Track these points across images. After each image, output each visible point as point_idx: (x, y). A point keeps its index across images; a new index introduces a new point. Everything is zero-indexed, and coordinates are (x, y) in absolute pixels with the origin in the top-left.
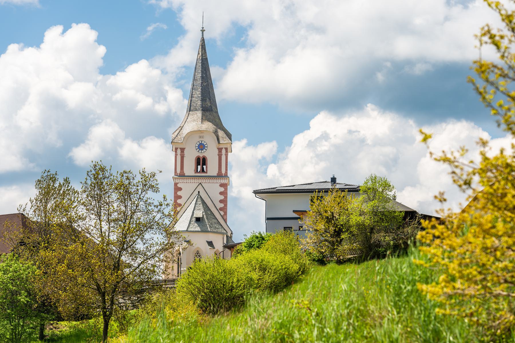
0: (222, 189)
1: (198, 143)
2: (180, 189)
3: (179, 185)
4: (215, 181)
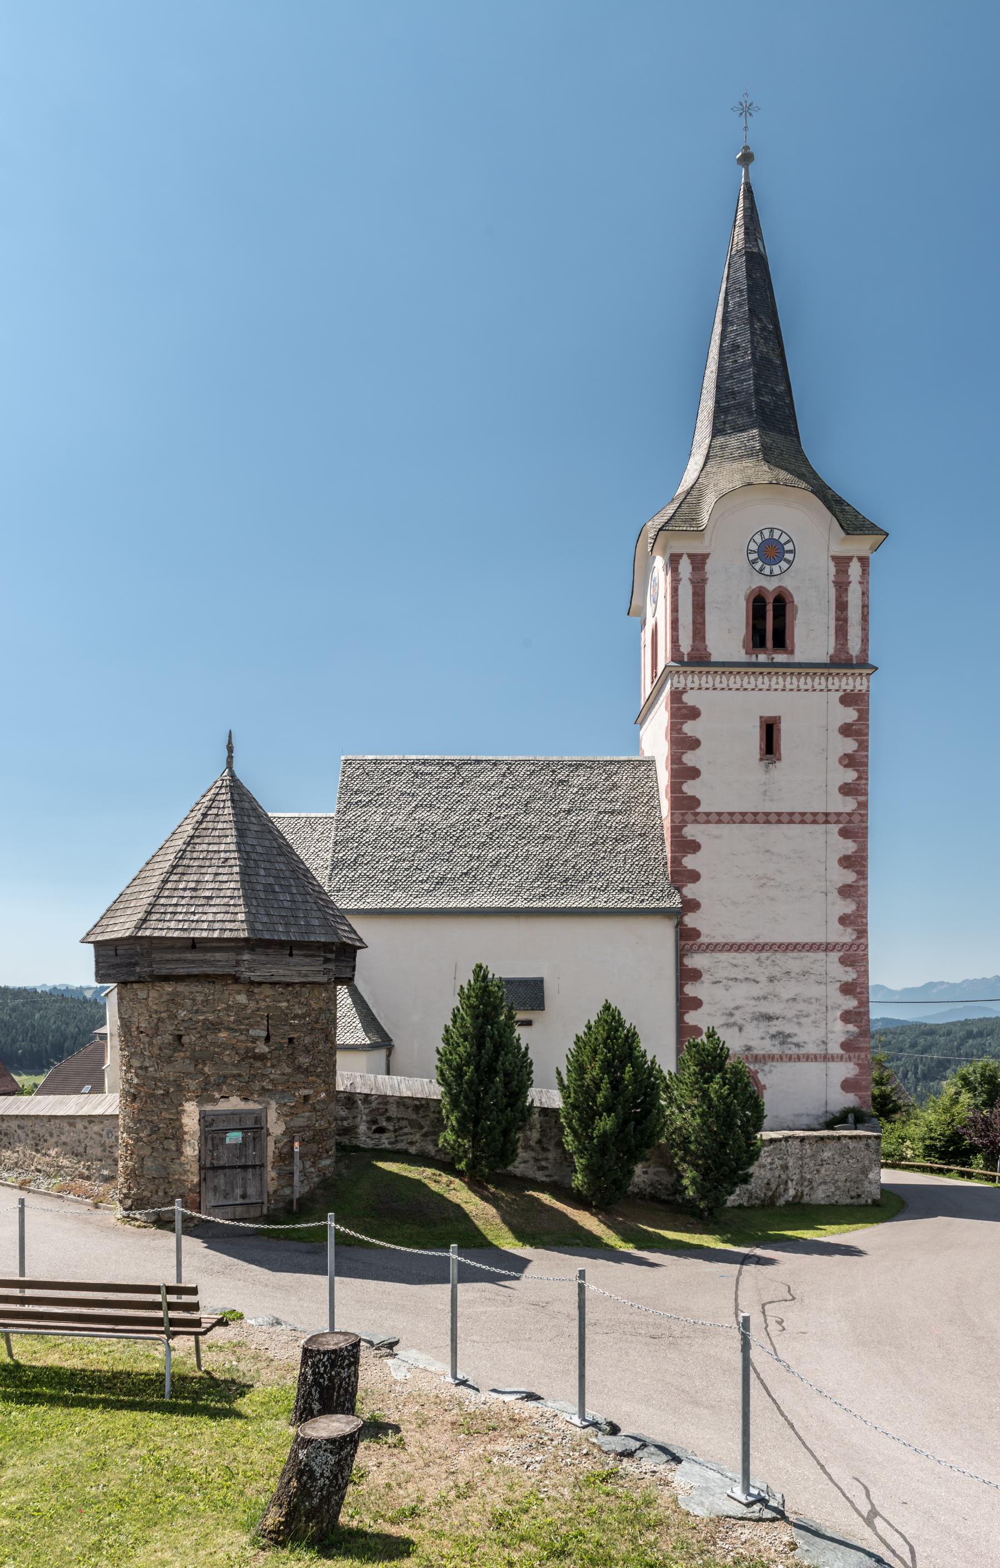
0: (850, 715)
1: (758, 539)
2: (694, 713)
3: (689, 699)
4: (819, 682)
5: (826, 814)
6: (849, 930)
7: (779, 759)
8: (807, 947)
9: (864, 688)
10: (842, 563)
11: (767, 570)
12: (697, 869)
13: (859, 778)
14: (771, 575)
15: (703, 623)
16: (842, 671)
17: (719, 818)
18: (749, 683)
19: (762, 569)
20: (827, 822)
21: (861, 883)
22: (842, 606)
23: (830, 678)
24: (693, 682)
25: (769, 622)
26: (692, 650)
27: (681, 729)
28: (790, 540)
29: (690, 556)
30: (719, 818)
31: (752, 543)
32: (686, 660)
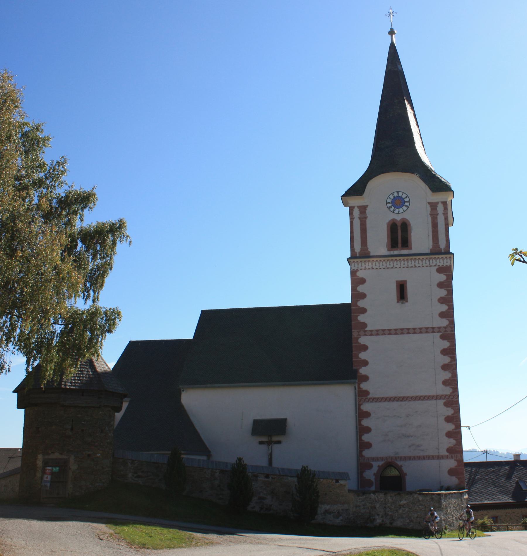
0: (442, 277)
1: (391, 197)
2: (363, 281)
3: (360, 274)
4: (426, 263)
5: (433, 328)
6: (448, 388)
7: (407, 301)
8: (426, 398)
9: (448, 264)
10: (433, 206)
11: (397, 211)
12: (367, 359)
13: (449, 309)
14: (399, 213)
15: (366, 238)
16: (437, 256)
17: (377, 333)
18: (390, 265)
19: (394, 210)
20: (433, 332)
21: (453, 363)
22: (435, 226)
23: (431, 260)
24: (362, 266)
25: (399, 236)
26: (361, 251)
27: (356, 289)
28: (407, 196)
29: (358, 207)
30: (377, 333)
31: (389, 199)
32: (358, 255)
